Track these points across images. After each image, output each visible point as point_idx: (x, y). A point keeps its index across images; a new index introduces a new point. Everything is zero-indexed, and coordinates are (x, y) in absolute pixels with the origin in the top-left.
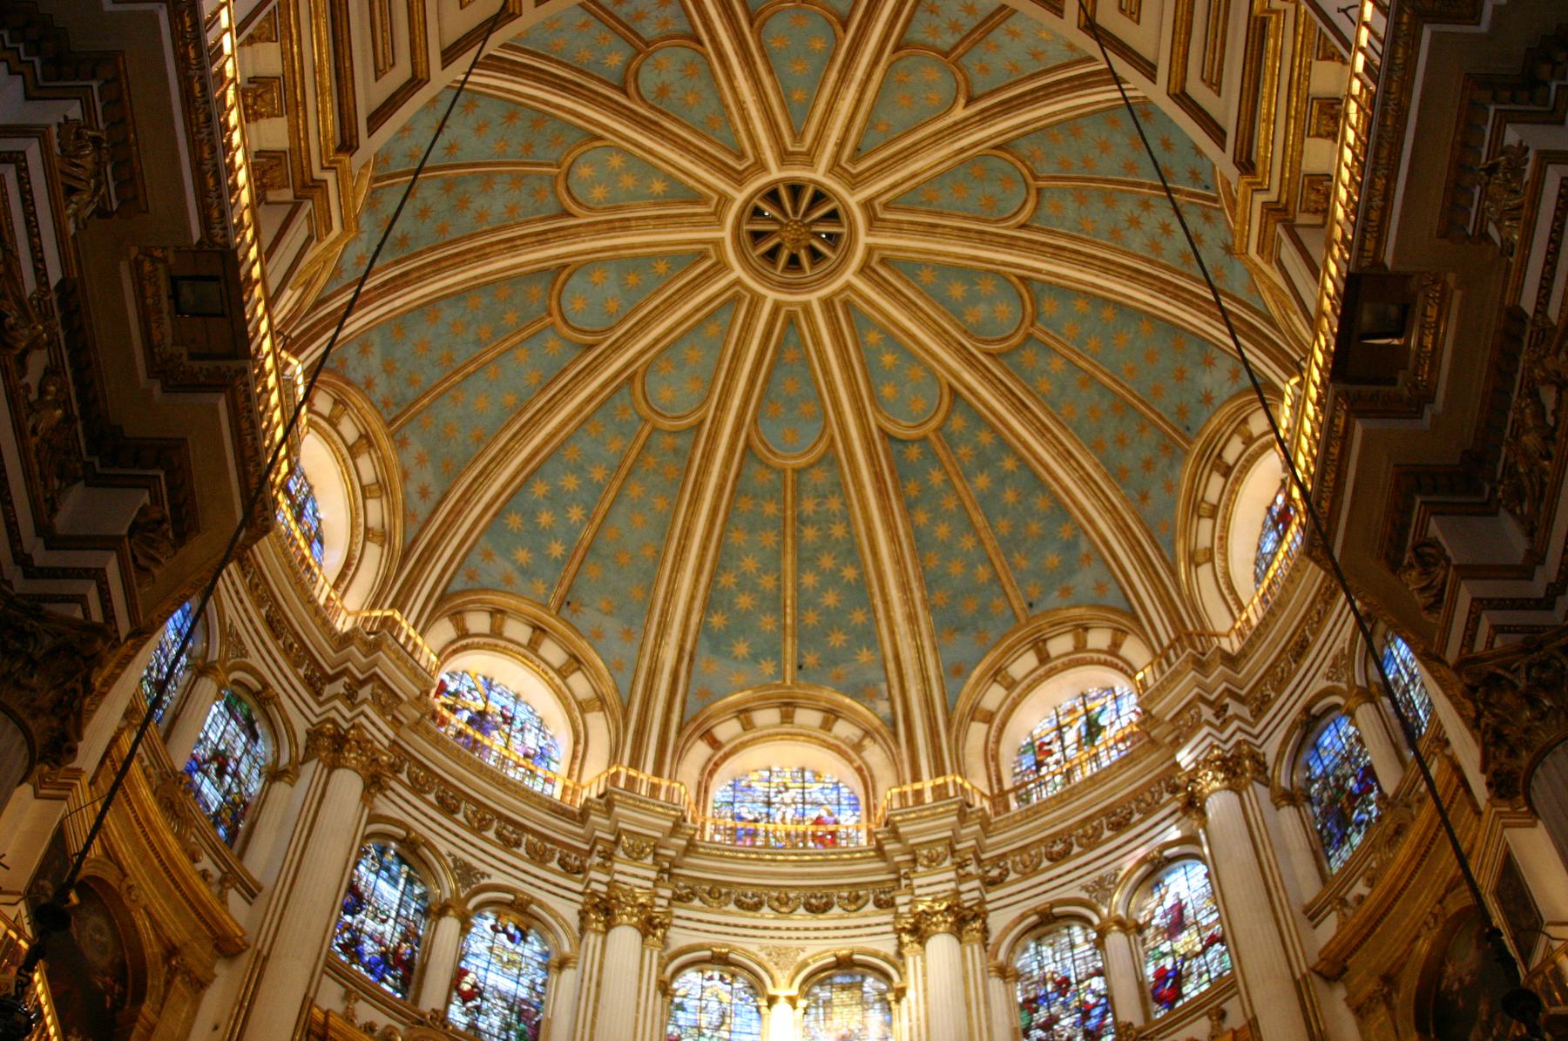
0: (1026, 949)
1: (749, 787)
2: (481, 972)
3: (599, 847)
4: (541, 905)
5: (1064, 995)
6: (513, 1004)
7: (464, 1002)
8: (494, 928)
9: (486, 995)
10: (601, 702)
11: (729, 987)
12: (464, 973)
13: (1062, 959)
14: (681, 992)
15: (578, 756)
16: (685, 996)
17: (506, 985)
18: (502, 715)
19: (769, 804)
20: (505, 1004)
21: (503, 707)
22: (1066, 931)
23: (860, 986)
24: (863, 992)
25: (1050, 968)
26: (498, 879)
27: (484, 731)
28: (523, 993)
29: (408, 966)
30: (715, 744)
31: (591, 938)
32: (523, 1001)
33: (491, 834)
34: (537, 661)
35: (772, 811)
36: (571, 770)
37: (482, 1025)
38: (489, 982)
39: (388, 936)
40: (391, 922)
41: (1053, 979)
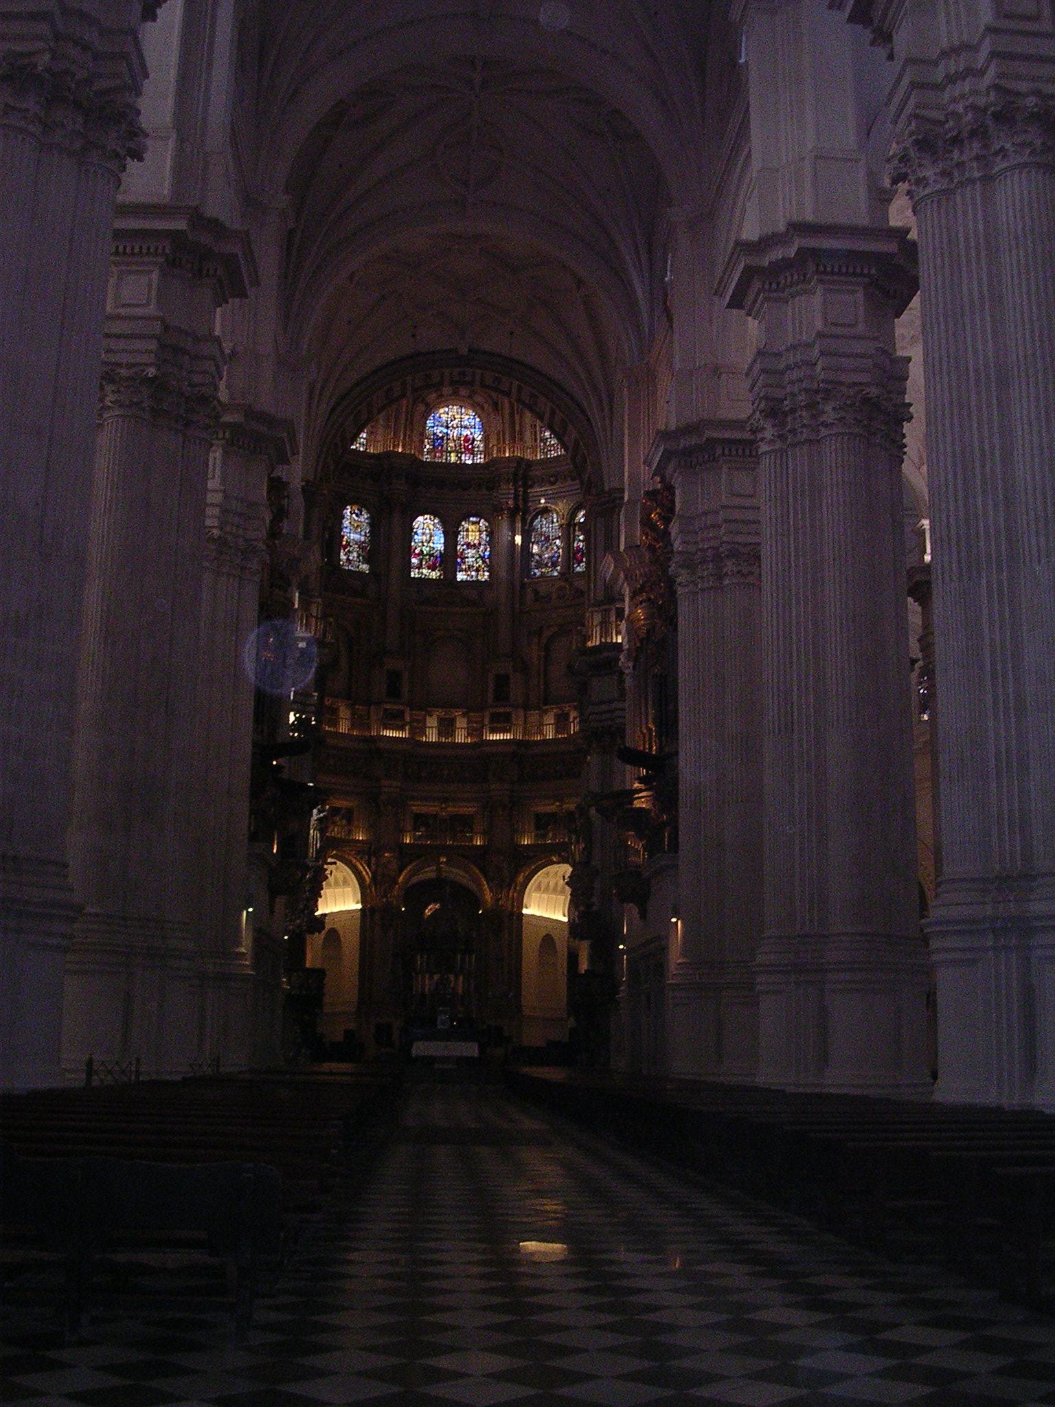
0: (537, 518)
1: (440, 417)
8: (350, 512)
12: (343, 537)
14: (416, 527)
17: (357, 537)
20: (357, 546)
23: (479, 523)
25: (544, 529)
28: (363, 539)
30: (427, 405)
32: (363, 542)
35: (449, 432)
37: (351, 558)
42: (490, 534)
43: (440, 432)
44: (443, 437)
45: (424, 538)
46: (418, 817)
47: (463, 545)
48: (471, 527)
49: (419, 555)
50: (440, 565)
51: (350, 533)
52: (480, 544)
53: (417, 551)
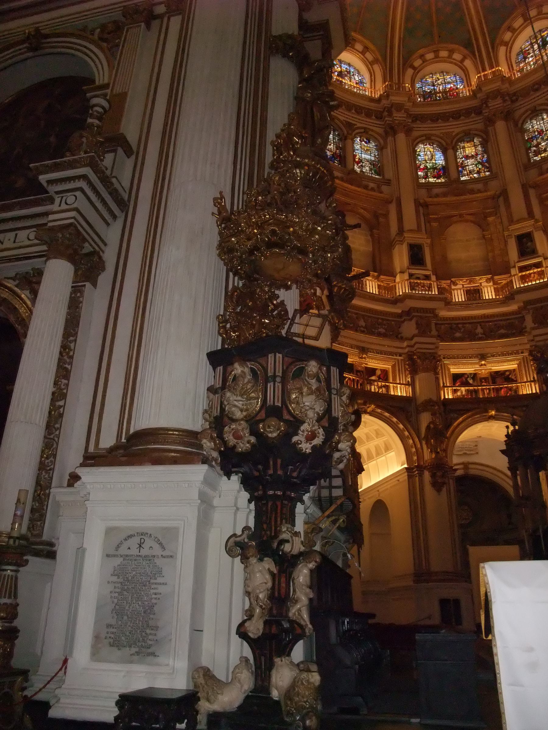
1: (426, 81)
2: (360, 155)
3: (386, 109)
4: (372, 131)
5: (542, 136)
6: (371, 162)
7: (358, 165)
9: (363, 161)
10: (376, 61)
11: (432, 147)
12: (356, 156)
13: (540, 124)
14: (418, 150)
15: (373, 81)
16: (419, 152)
17: (368, 157)
18: (346, 71)
19: (434, 85)
21: (346, 68)
22: (540, 115)
24: (474, 142)
26: (359, 125)
27: (343, 78)
28: (373, 159)
29: (340, 156)
30: (414, 68)
31: (390, 139)
33: (353, 111)
34: (355, 51)
35: (435, 88)
36: (371, 85)
38: (363, 157)
39: (332, 149)
40: (332, 144)
41: (537, 131)
42: (484, 144)
43: (428, 89)
44: (430, 92)
45: (427, 158)
46: (457, 378)
47: (462, 158)
48: (466, 145)
49: (423, 169)
50: (444, 174)
51: (361, 154)
52: (477, 154)
53: (422, 167)
